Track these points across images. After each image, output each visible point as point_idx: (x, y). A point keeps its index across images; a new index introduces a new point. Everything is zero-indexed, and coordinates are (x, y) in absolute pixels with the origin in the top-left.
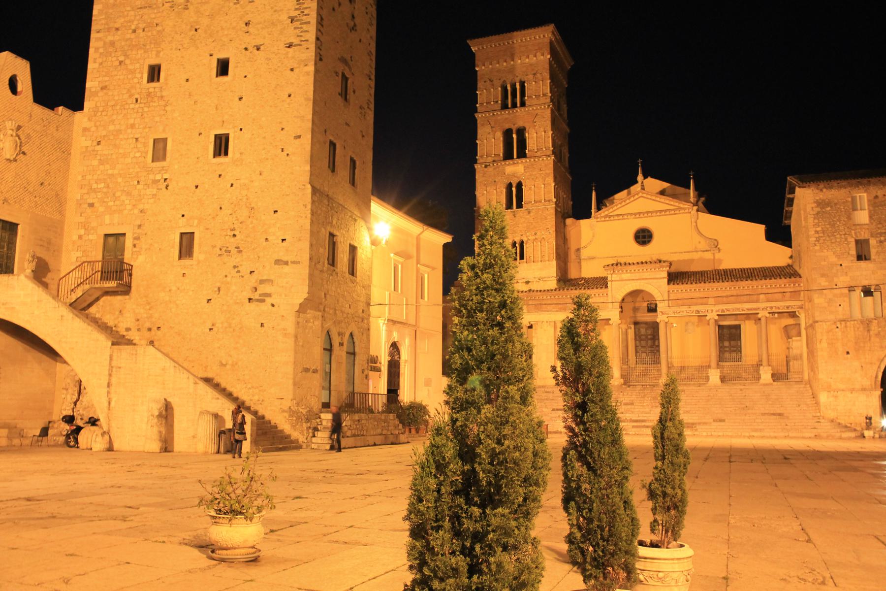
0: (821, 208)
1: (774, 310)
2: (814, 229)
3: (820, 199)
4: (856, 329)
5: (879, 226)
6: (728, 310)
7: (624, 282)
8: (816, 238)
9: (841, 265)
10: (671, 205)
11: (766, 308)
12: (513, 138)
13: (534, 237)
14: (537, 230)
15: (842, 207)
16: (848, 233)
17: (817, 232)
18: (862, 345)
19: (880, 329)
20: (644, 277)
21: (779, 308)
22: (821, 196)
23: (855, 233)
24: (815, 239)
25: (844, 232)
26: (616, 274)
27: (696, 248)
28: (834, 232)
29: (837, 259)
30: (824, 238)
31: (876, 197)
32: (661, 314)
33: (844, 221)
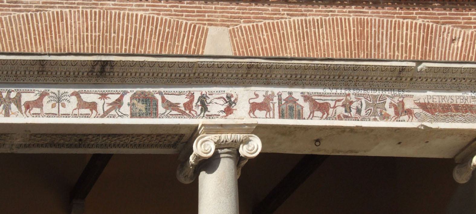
6: (323, 108)
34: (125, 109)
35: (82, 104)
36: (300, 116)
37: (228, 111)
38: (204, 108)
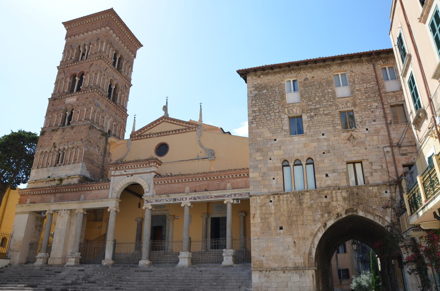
0: (258, 91)
1: (237, 197)
2: (252, 109)
3: (258, 84)
4: (289, 203)
5: (309, 103)
6: (200, 198)
7: (123, 177)
8: (253, 116)
9: (275, 140)
10: (183, 126)
11: (230, 195)
12: (76, 80)
13: (72, 146)
14: (75, 141)
15: (277, 89)
16: (281, 111)
17: (254, 112)
18: (294, 219)
19: (312, 202)
20: (138, 172)
21: (241, 195)
22: (259, 81)
23: (288, 111)
24: (252, 118)
25: (278, 111)
26: (118, 170)
27: (198, 156)
28: (269, 111)
29: (271, 134)
30: (261, 116)
31: (306, 79)
32: (146, 202)
33: (278, 101)
34: (172, 201)
35: (166, 200)
36: (196, 200)
37: (186, 200)
38: (183, 200)
